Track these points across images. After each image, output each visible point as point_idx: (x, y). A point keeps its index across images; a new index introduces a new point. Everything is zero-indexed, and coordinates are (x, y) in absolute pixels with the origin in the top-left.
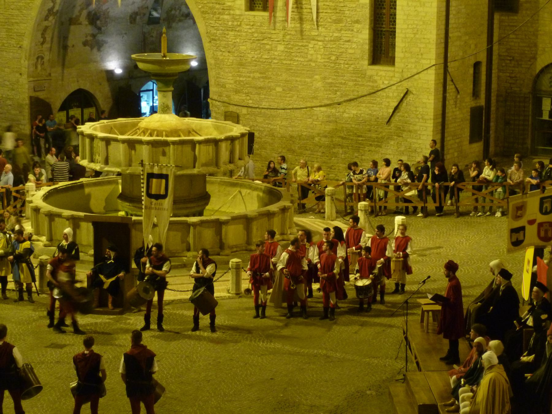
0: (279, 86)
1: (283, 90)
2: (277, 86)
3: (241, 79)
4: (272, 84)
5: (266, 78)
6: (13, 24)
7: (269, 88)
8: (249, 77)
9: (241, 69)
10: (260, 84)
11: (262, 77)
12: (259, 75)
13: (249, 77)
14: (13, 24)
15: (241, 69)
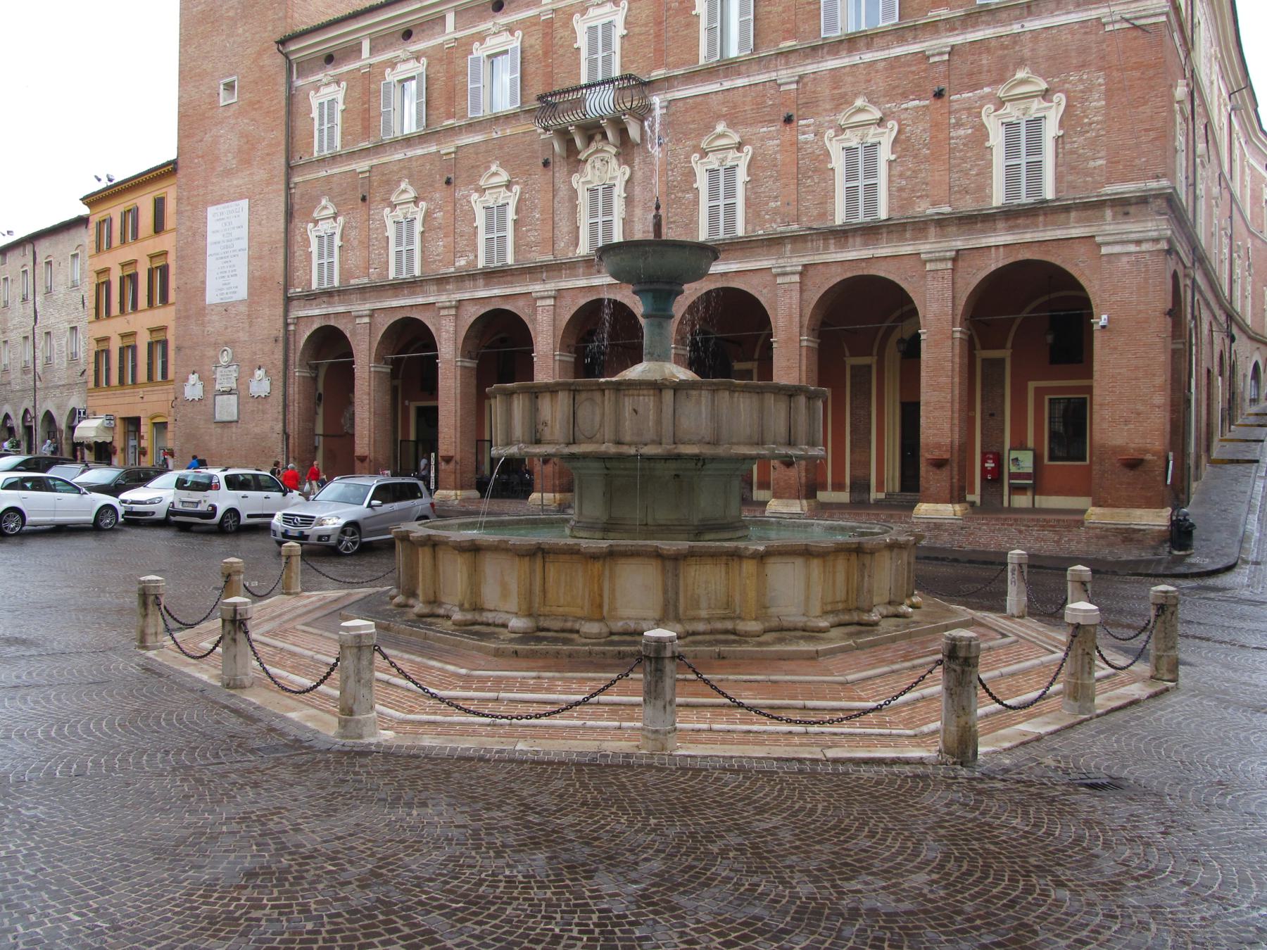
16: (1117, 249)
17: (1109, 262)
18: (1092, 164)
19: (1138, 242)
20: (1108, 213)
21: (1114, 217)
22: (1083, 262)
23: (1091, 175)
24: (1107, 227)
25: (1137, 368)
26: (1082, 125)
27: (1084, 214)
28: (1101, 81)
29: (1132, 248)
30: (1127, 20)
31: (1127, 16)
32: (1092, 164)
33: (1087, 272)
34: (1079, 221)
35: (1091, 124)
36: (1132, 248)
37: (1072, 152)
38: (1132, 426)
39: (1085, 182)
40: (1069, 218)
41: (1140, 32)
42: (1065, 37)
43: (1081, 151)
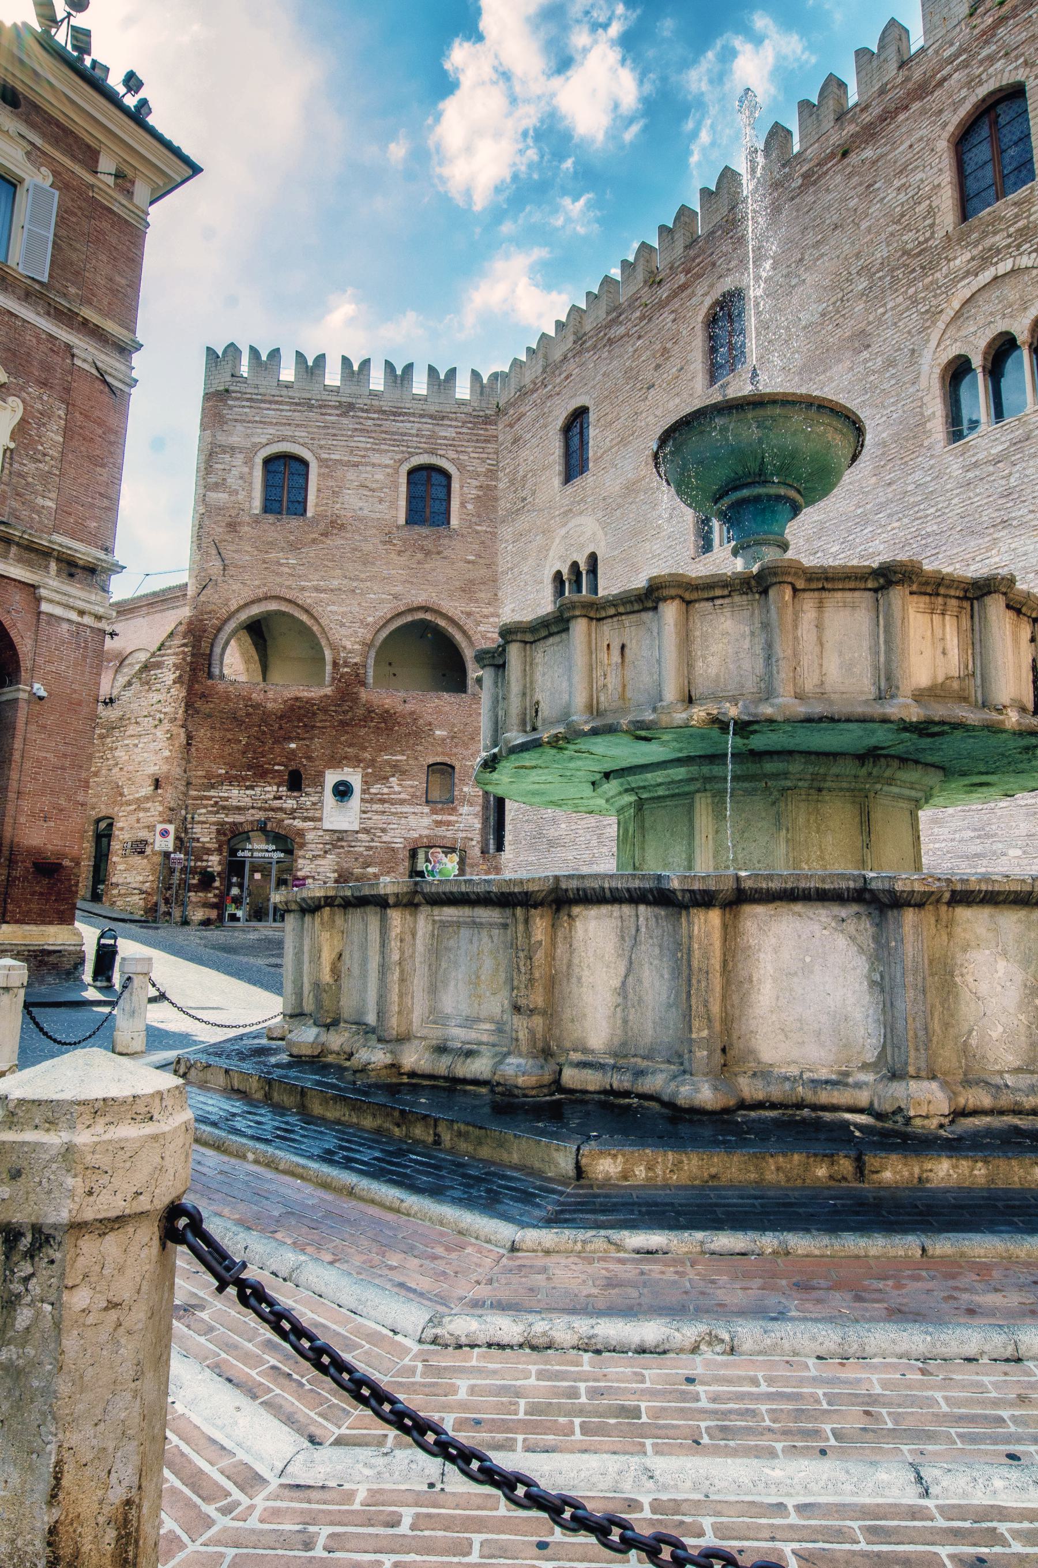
0: (1016, 847)
1: (1024, 852)
2: (1011, 846)
3: (937, 846)
4: (1000, 846)
5: (988, 836)
6: (605, 826)
7: (994, 853)
8: (953, 840)
9: (936, 830)
10: (976, 848)
11: (979, 837)
12: (972, 834)
13: (953, 840)
14: (605, 826)
15: (936, 830)
16: (58, 611)
17: (48, 623)
18: (40, 501)
19: (82, 613)
20: (53, 566)
21: (59, 571)
22: (18, 612)
23: (39, 513)
24: (51, 582)
25: (65, 756)
26: (36, 450)
27: (26, 555)
28: (61, 413)
29: (74, 616)
30: (97, 369)
31: (99, 364)
32: (40, 501)
33: (19, 625)
34: (20, 560)
35: (45, 455)
36: (74, 616)
37: (20, 475)
38: (52, 824)
39: (32, 519)
40: (8, 551)
41: (107, 389)
42: (29, 338)
43: (30, 480)
